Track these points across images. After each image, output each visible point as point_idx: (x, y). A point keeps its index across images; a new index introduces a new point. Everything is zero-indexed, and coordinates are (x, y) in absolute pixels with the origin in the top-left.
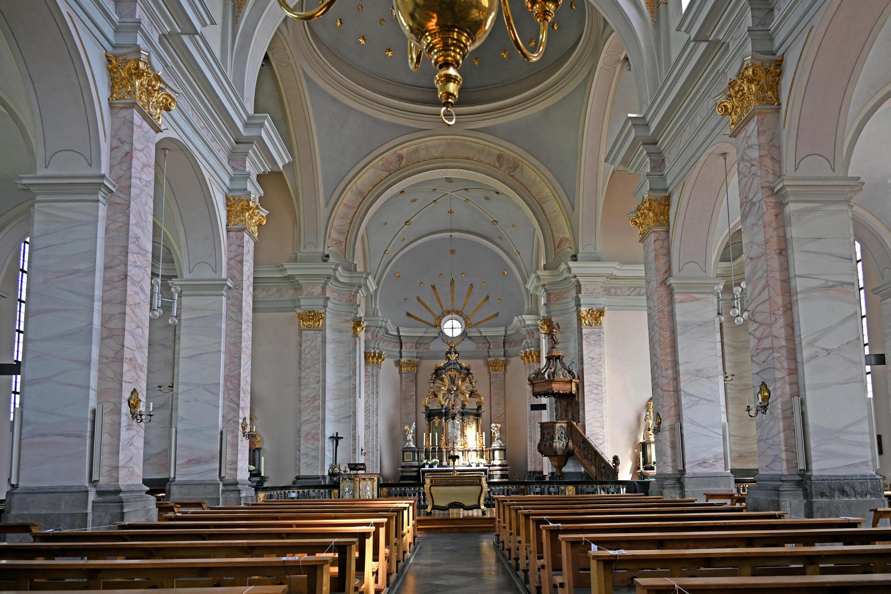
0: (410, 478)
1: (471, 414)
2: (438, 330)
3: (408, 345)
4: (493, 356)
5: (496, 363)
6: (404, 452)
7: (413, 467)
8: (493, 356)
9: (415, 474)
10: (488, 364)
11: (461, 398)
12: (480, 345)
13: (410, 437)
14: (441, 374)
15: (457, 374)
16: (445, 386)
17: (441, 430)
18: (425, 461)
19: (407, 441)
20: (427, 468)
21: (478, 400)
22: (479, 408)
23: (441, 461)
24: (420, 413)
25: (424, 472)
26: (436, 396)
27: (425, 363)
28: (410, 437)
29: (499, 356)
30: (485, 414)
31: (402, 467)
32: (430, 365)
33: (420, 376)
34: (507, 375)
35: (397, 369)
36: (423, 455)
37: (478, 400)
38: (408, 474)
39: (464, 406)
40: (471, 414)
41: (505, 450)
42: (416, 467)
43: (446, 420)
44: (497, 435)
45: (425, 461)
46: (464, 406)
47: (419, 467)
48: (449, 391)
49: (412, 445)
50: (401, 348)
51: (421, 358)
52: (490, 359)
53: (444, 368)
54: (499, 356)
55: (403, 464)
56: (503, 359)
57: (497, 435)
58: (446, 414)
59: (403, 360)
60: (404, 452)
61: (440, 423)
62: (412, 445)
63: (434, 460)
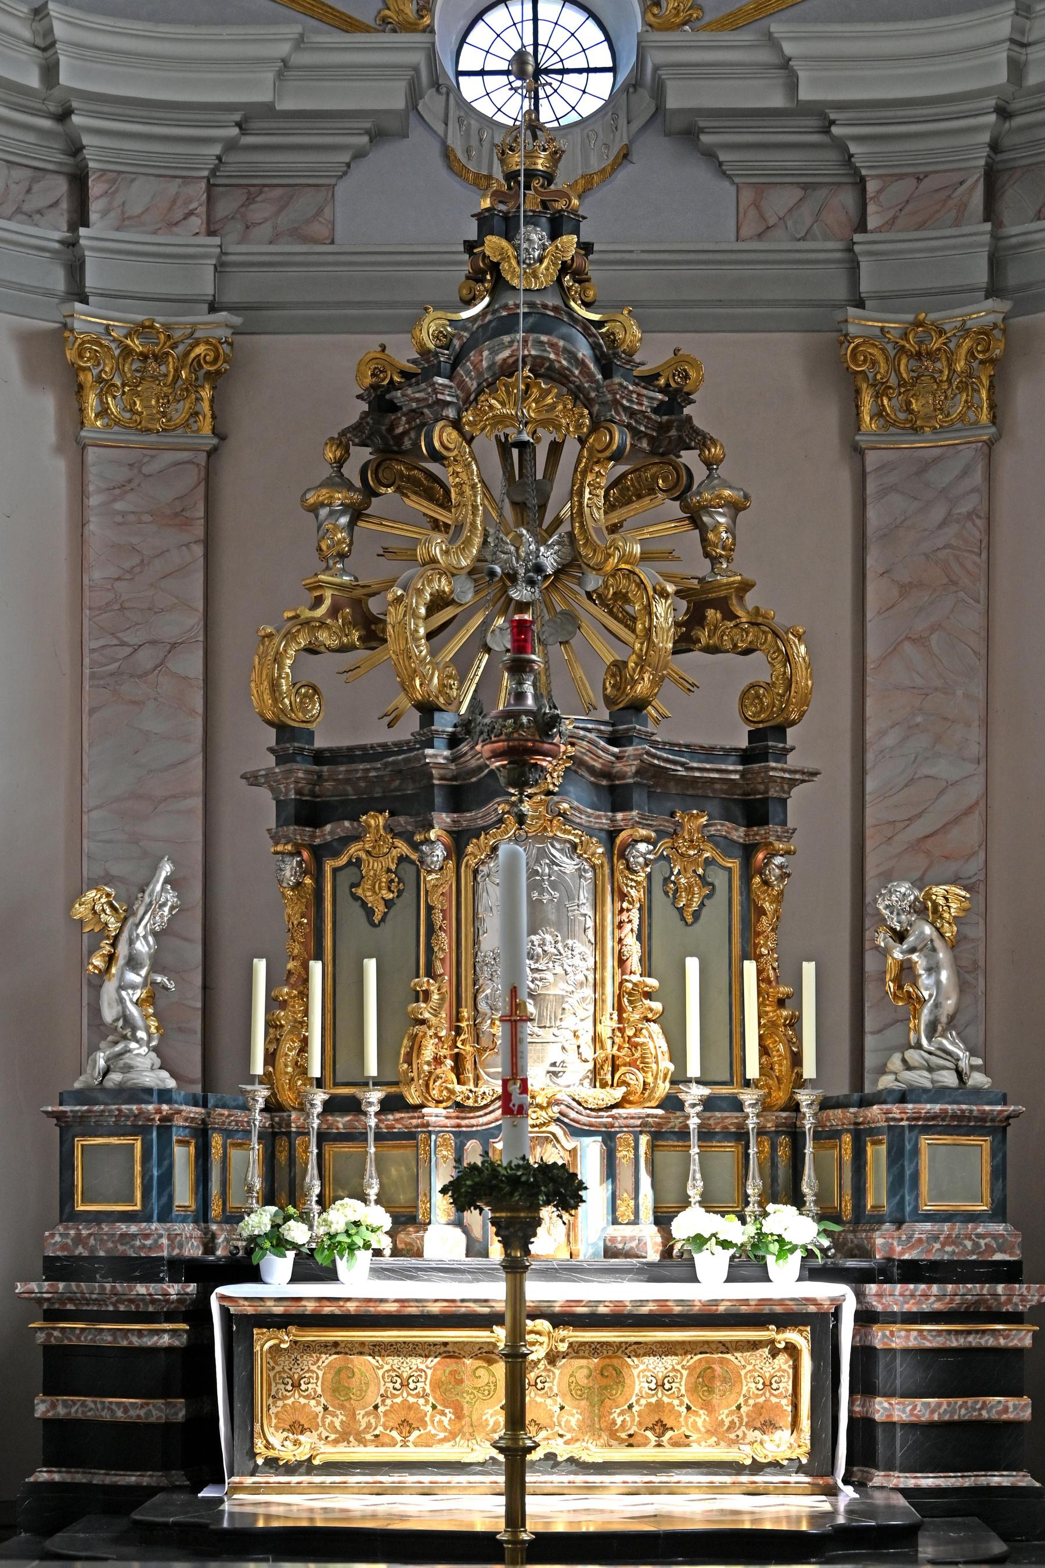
0: (126, 1370)
1: (694, 792)
2: (403, 51)
3: (139, 195)
4: (887, 299)
5: (919, 352)
6: (69, 1128)
7: (147, 1268)
8: (887, 299)
9: (166, 1336)
10: (844, 375)
11: (599, 643)
12: (779, 202)
13: (125, 994)
14: (421, 423)
15: (572, 420)
16: (453, 532)
17: (426, 948)
18: (260, 1220)
19: (100, 1030)
20: (278, 1276)
21: (757, 668)
22: (766, 740)
23: (407, 1219)
24: (233, 788)
25: (242, 1326)
26: (372, 631)
27: (279, 353)
28: (125, 994)
29: (960, 293)
30: (812, 812)
31: (56, 1268)
32: (318, 378)
33: (245, 473)
34: (1008, 460)
35: (47, 404)
36: (249, 1164)
37: (757, 668)
38: (106, 1334)
39: (625, 715)
40: (694, 792)
41: (997, 1129)
42: (183, 1269)
43: (459, 841)
44: (937, 984)
45: (260, 1220)
46: (625, 715)
47: (210, 1273)
48: (492, 580)
49: (145, 1068)
50: (80, 217)
51: (256, 316)
52: (861, 323)
53: (453, 355)
54: (960, 293)
55: (58, 1241)
56: (984, 312)
57: (937, 984)
58: (451, 786)
59: (86, 319)
60: (69, 1128)
61: (409, 871)
62: (145, 1068)
63: (343, 1213)
